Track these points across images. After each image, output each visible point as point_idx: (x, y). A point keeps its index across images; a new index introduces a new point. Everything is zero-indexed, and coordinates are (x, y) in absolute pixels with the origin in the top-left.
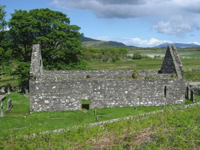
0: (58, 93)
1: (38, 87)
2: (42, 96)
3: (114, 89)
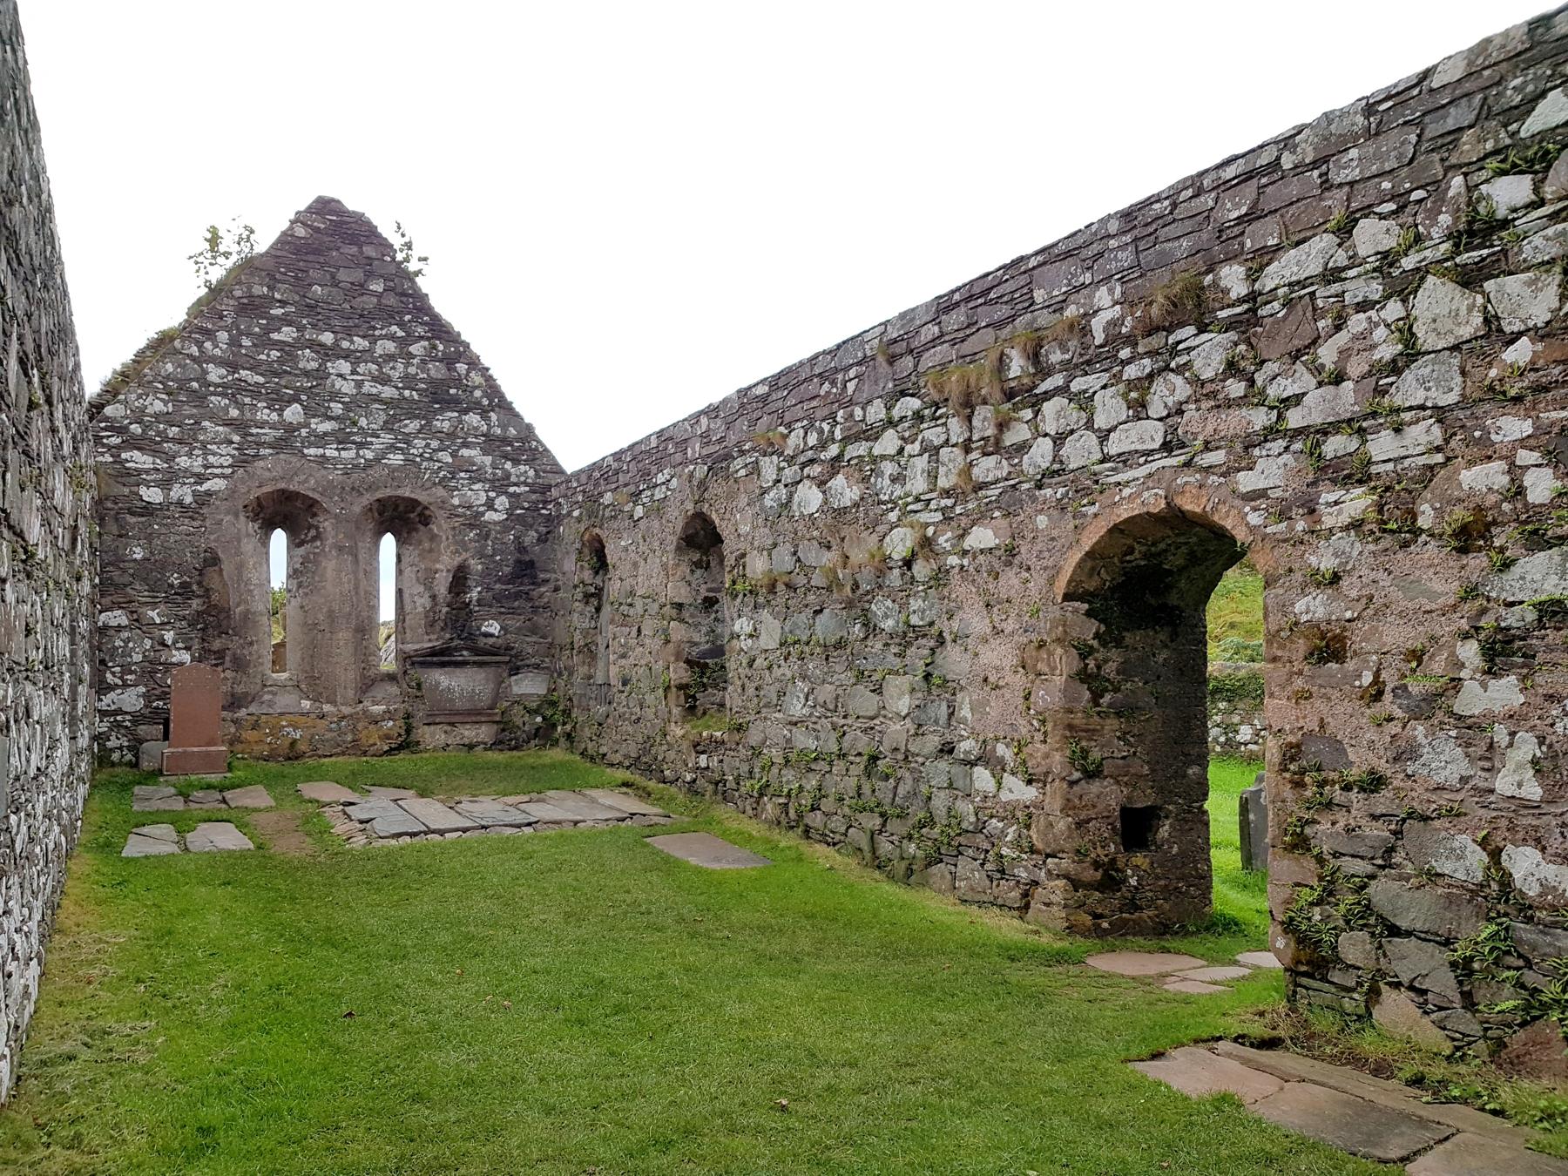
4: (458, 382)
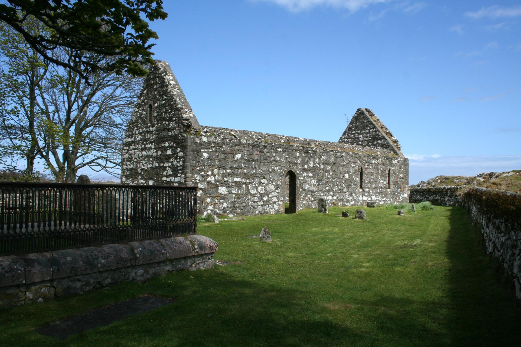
0: (245, 171)
1: (207, 152)
2: (214, 176)
3: (332, 167)
4: (377, 135)
